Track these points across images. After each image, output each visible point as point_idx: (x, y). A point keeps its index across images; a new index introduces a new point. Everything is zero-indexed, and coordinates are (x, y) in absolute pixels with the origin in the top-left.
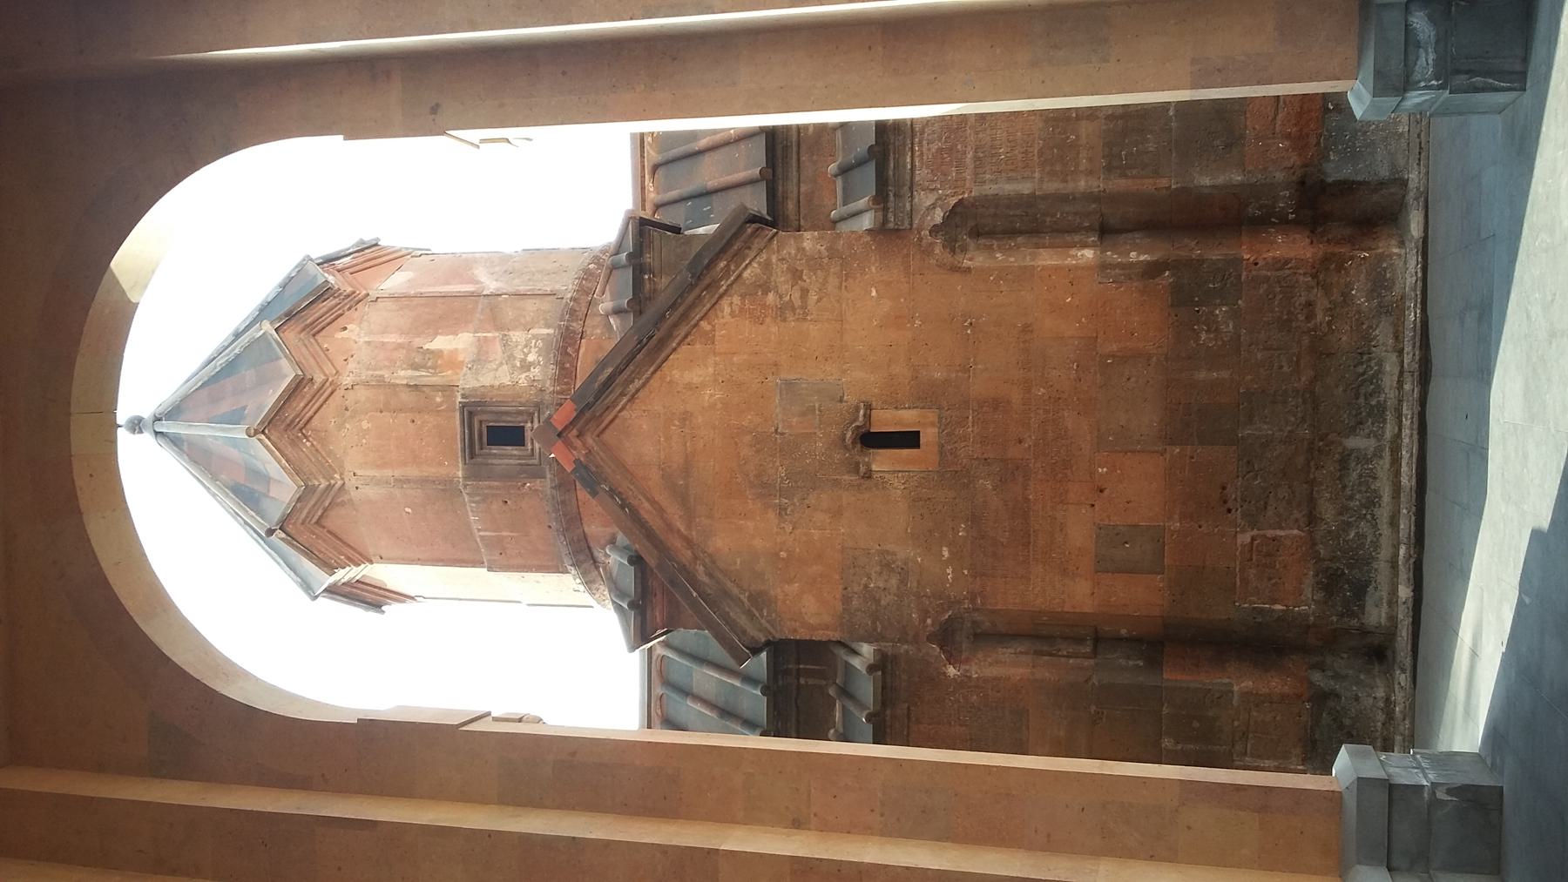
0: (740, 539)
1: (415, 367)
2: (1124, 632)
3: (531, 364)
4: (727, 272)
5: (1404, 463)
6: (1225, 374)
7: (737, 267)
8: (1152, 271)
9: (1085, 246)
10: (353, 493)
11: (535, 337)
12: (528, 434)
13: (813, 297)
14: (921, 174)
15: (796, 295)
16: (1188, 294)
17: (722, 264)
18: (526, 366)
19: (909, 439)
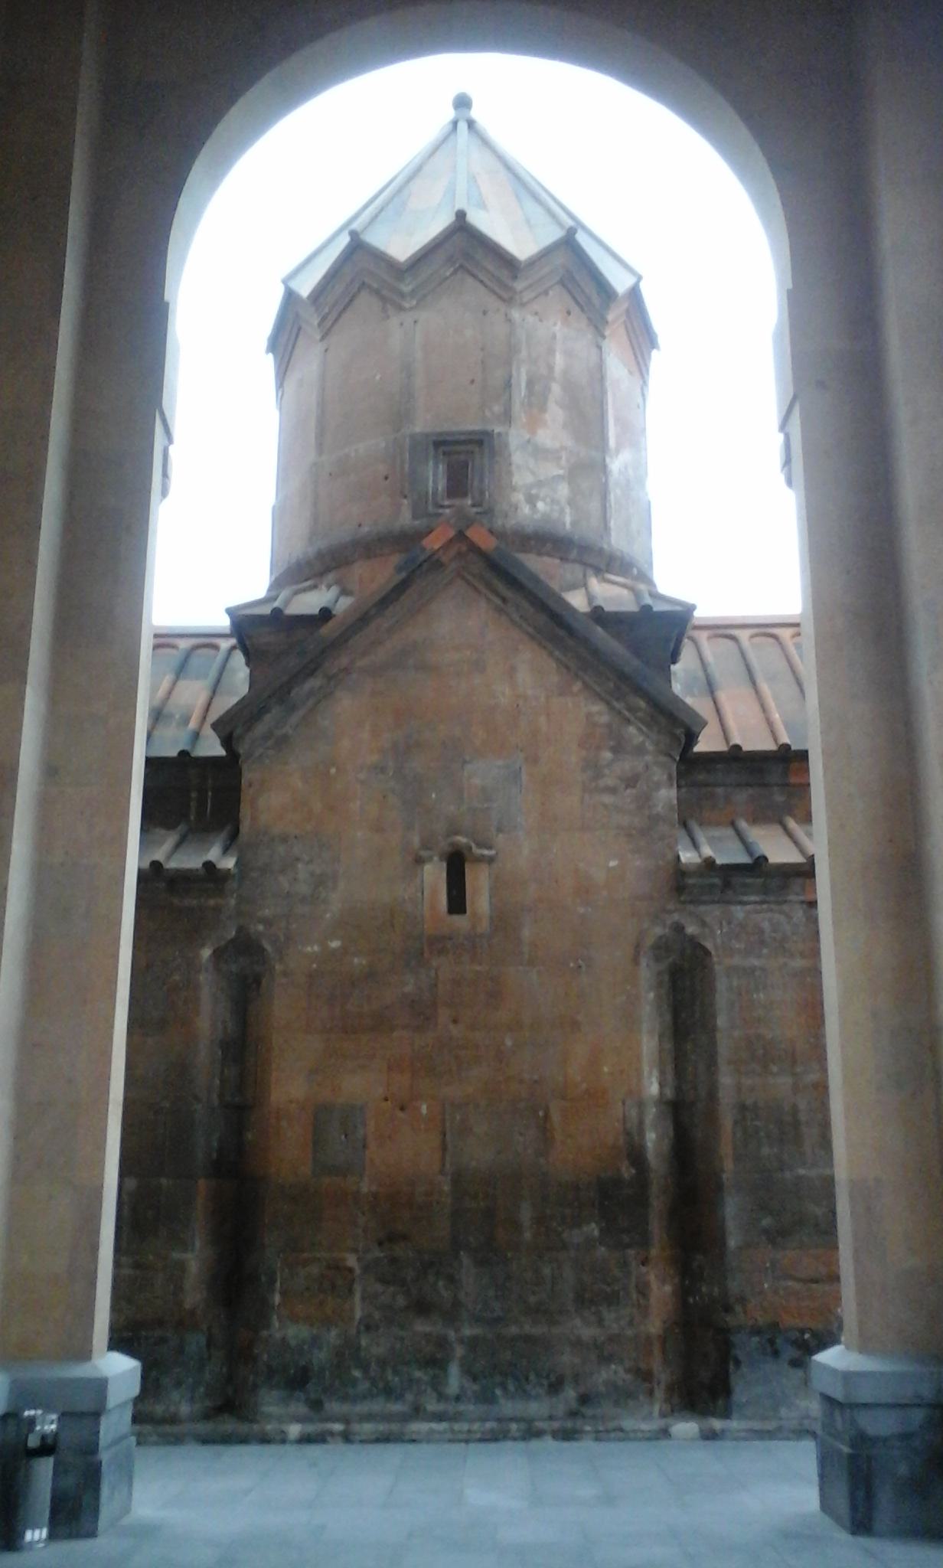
0: (349, 725)
1: (530, 383)
2: (249, 1136)
3: (534, 506)
4: (630, 709)
5: (434, 1426)
6: (528, 1235)
7: (641, 720)
8: (636, 1156)
9: (661, 1085)
10: (394, 321)
11: (562, 511)
12: (457, 502)
13: (608, 799)
14: (739, 912)
15: (609, 781)
16: (614, 1199)
17: (642, 704)
18: (532, 500)
19: (457, 903)
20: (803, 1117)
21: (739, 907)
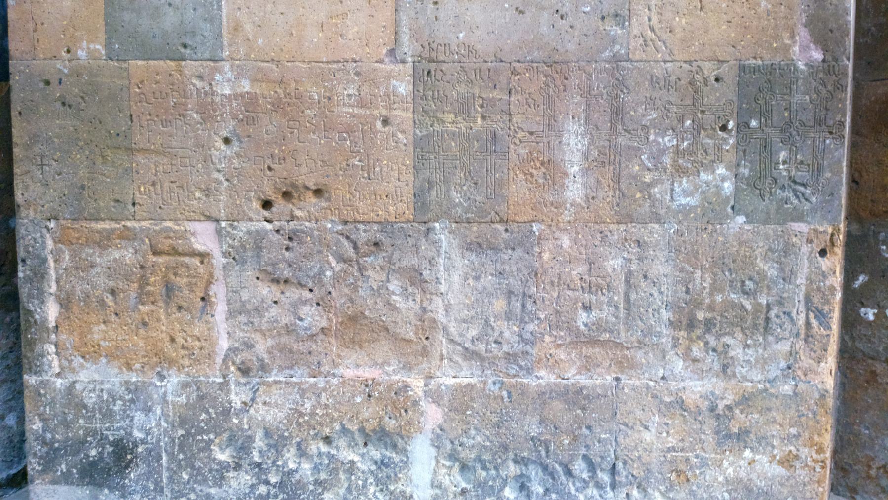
6: (575, 191)
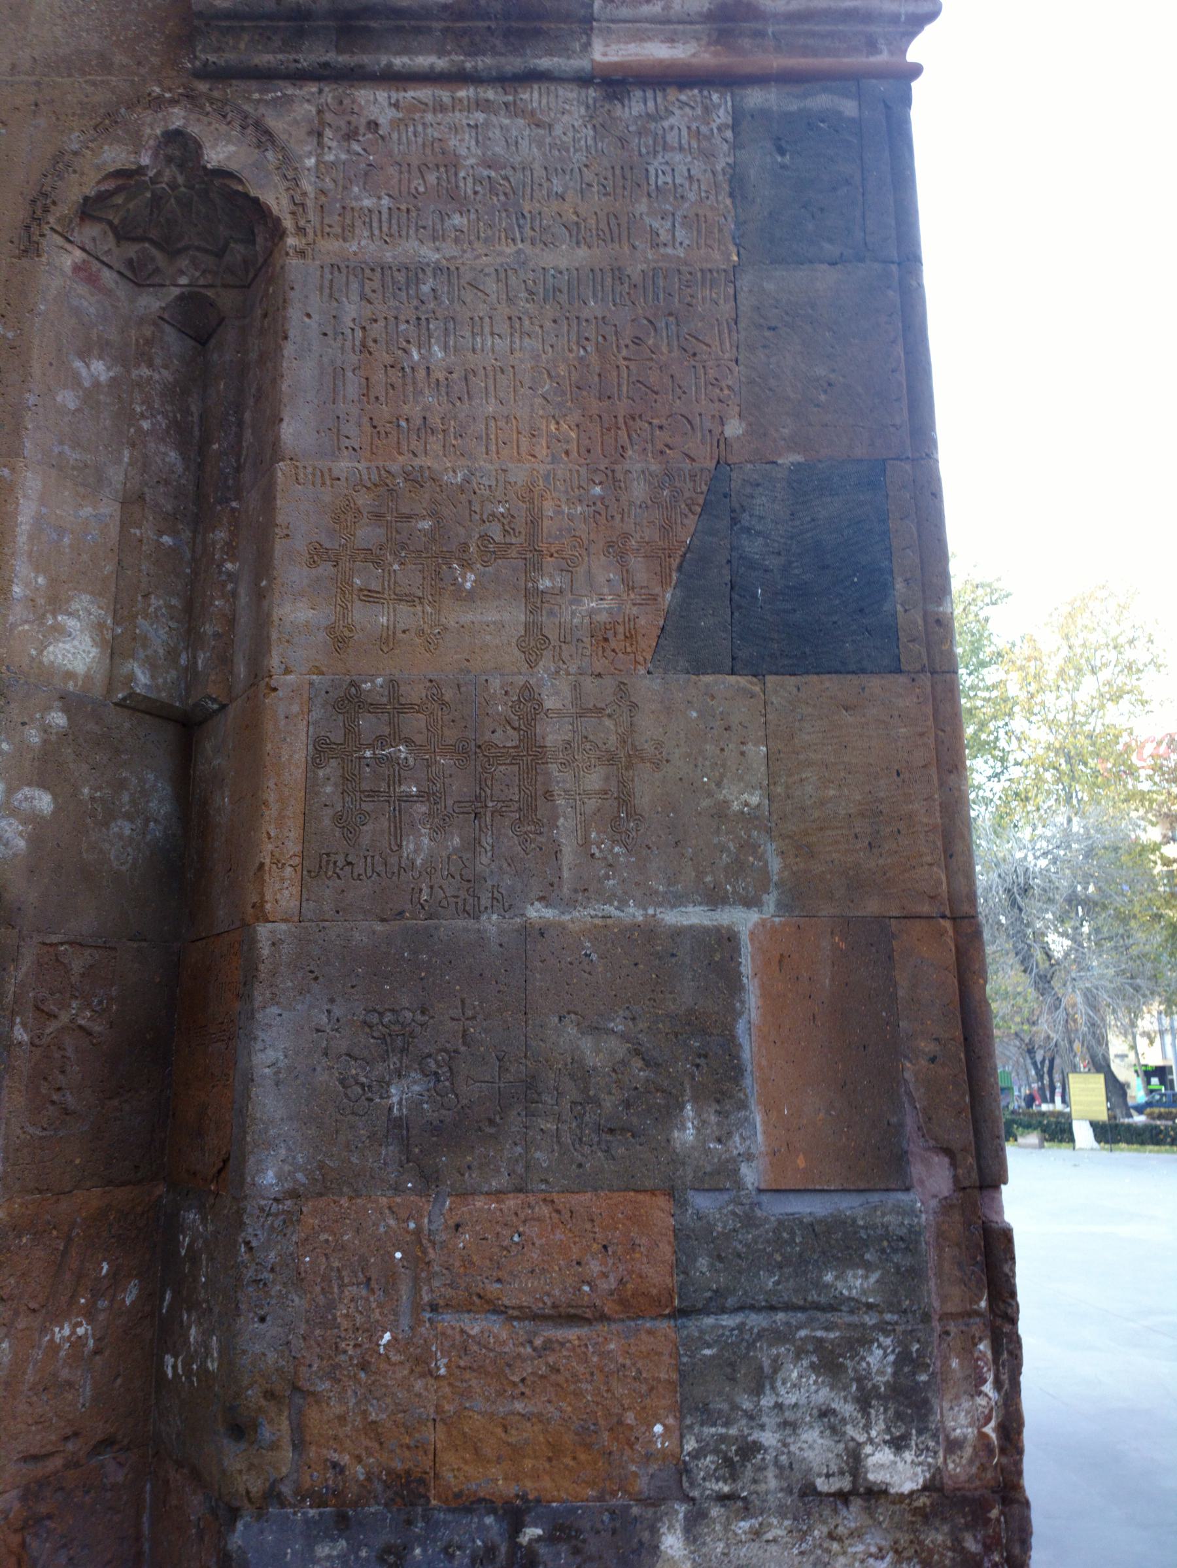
20: (553, 734)
21: (382, 95)
